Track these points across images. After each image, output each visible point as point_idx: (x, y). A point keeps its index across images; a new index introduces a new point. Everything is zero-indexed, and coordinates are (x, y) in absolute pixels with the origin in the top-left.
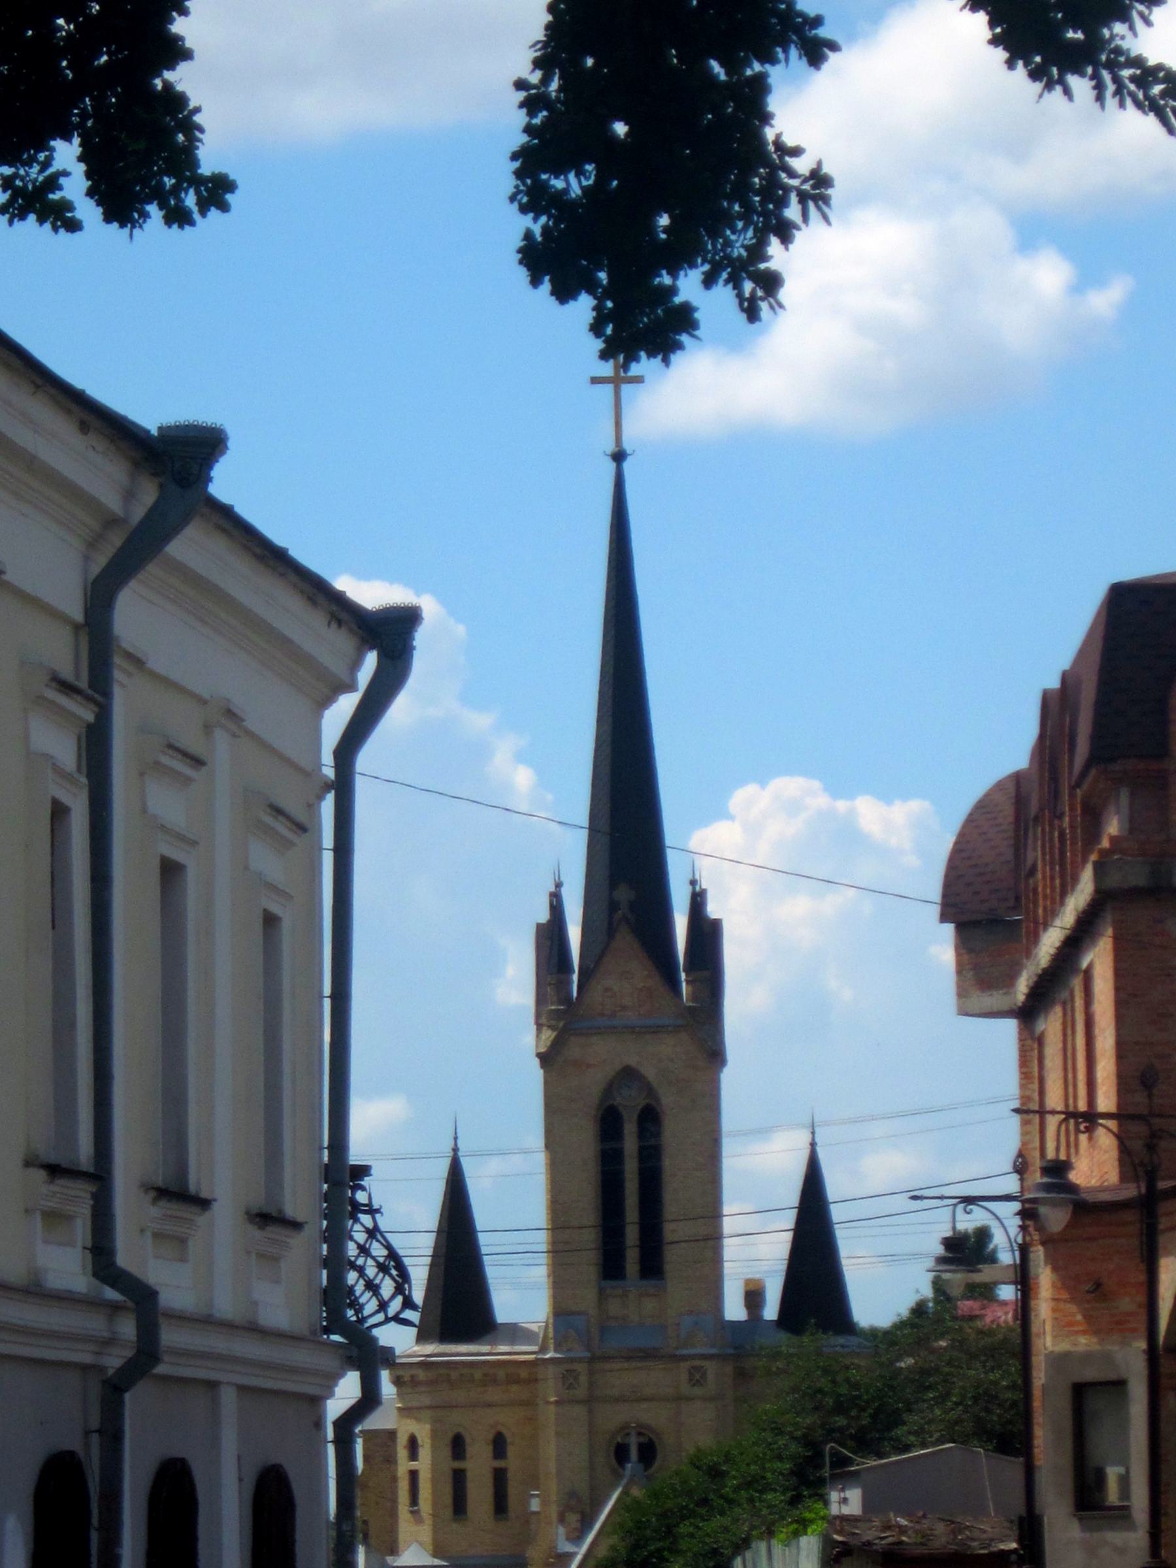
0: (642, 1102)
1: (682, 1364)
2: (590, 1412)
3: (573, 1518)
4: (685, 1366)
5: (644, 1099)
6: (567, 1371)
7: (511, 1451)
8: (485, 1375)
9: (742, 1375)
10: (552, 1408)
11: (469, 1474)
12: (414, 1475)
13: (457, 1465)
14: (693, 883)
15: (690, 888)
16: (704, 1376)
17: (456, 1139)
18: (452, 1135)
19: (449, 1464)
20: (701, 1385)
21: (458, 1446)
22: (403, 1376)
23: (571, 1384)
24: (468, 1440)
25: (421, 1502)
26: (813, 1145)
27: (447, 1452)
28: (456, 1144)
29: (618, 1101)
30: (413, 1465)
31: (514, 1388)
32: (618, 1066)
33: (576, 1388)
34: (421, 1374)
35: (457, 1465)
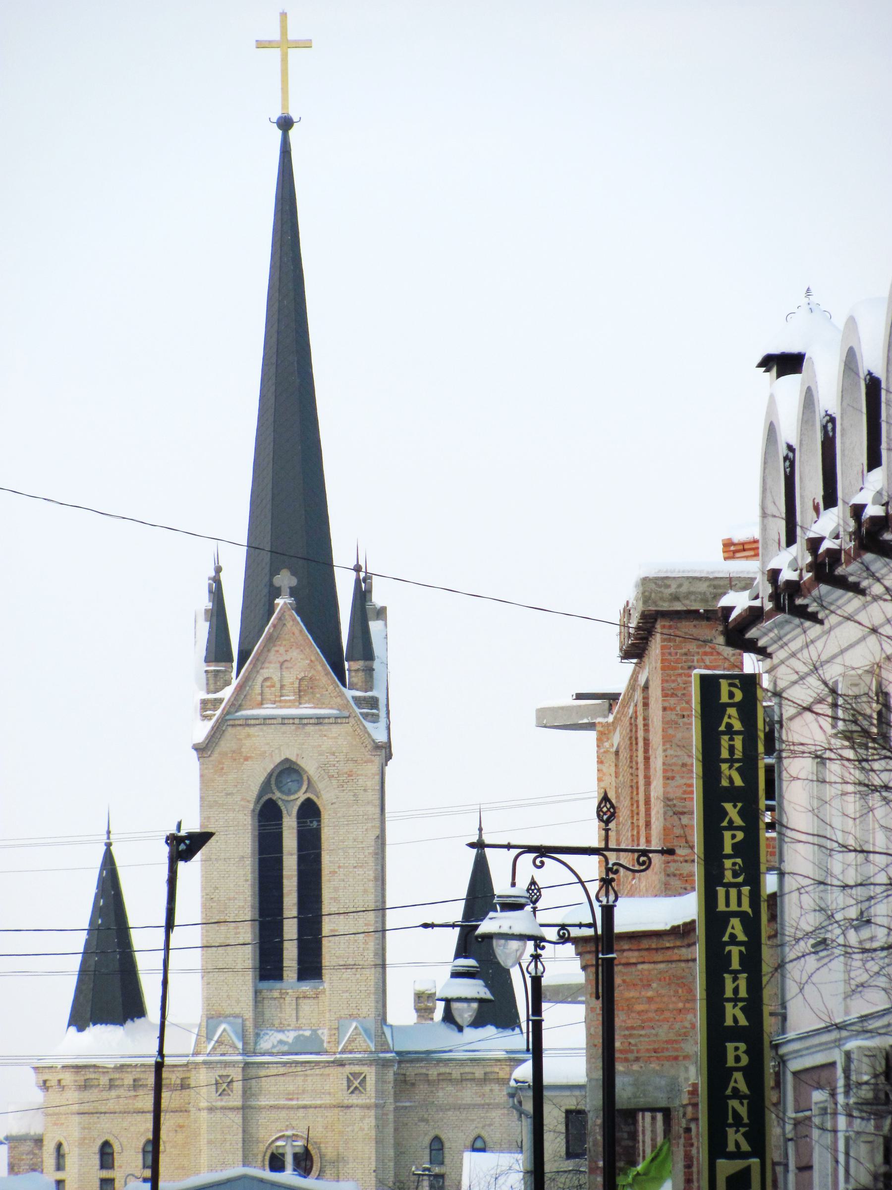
0: (301, 796)
2: (244, 1119)
5: (305, 792)
6: (219, 1076)
8: (135, 1080)
9: (403, 1084)
10: (204, 1114)
13: (106, 1174)
18: (106, 829)
20: (361, 1092)
21: (106, 1155)
23: (224, 1090)
24: (116, 1148)
29: (277, 795)
30: (60, 1175)
32: (278, 760)
33: (229, 1095)
34: (68, 1078)
35: (106, 1174)
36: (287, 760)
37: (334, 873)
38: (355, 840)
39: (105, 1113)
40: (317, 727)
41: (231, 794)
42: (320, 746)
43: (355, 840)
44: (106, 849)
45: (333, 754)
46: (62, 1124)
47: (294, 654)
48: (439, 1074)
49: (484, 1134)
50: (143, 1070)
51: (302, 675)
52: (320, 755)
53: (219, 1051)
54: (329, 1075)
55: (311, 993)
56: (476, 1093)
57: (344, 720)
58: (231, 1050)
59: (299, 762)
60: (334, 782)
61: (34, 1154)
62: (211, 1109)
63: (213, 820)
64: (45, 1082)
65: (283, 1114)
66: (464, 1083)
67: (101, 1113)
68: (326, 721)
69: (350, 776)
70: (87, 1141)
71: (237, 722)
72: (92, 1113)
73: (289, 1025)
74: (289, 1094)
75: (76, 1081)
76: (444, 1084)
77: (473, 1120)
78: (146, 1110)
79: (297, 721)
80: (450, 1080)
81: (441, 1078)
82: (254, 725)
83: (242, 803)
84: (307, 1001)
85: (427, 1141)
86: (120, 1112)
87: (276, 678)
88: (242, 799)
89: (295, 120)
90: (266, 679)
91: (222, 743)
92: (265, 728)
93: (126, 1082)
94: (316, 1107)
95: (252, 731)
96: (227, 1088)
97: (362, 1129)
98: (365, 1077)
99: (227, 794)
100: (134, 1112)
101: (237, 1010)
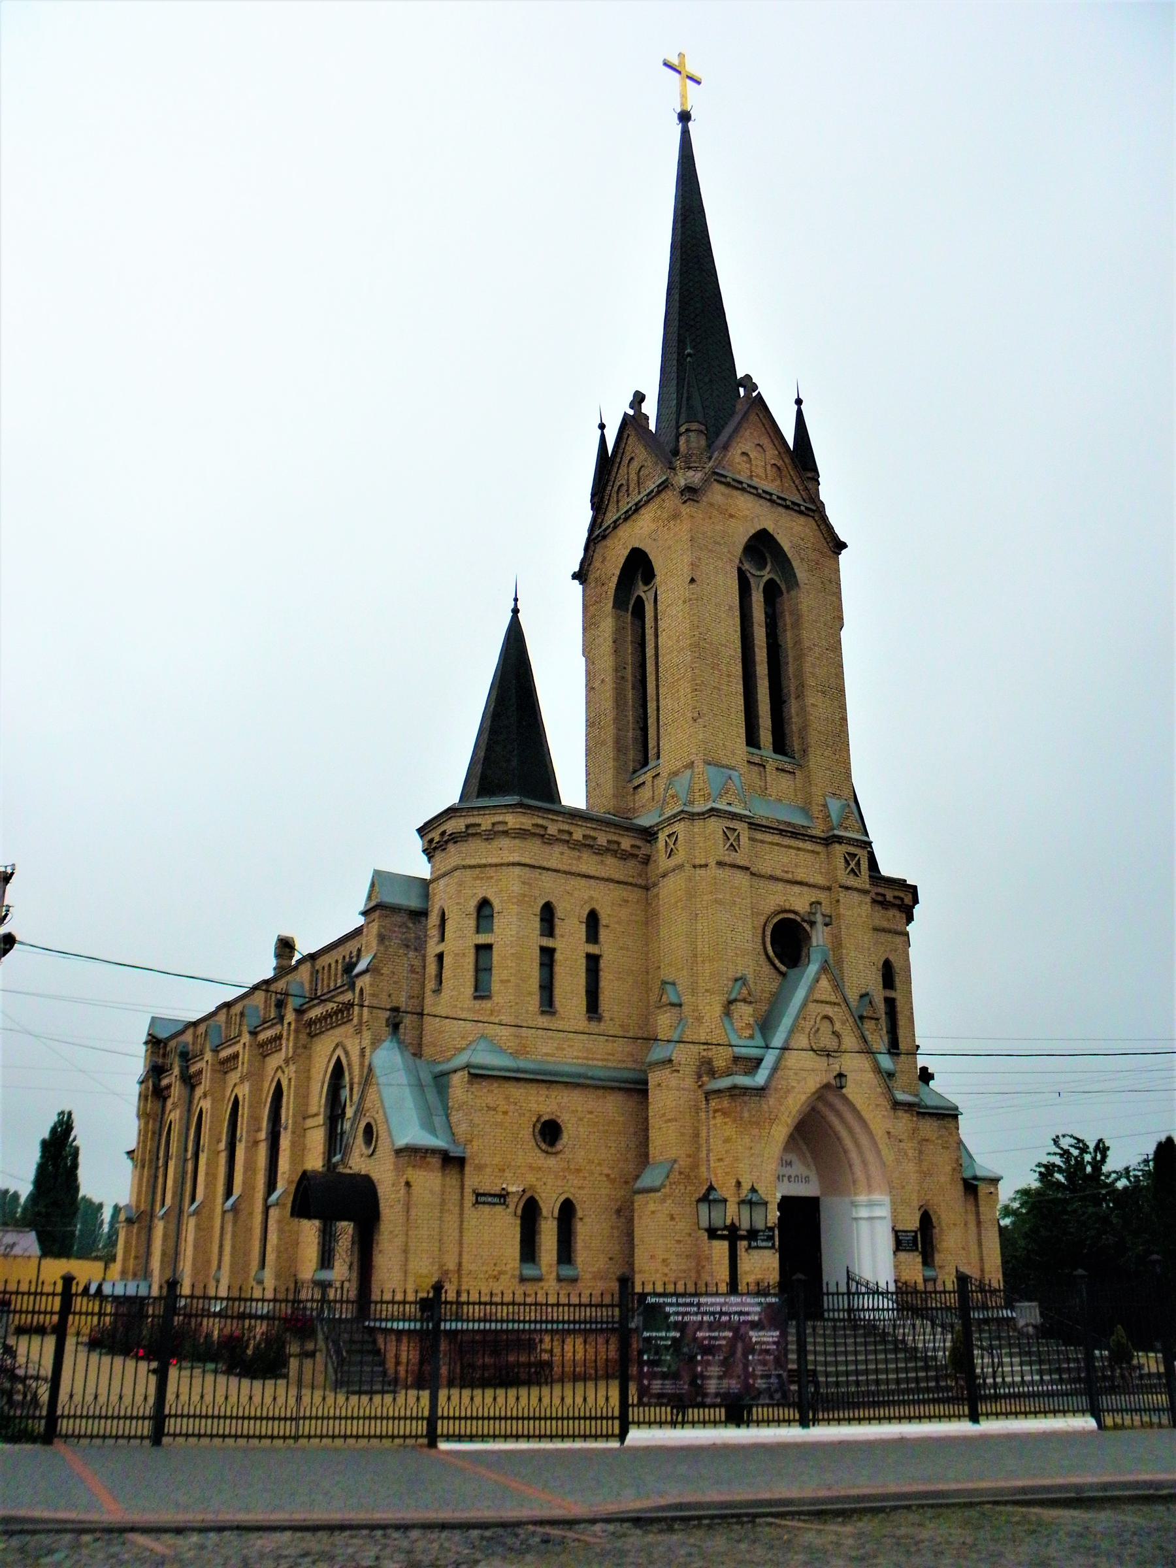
0: (767, 574)
1: (837, 846)
3: (744, 1012)
4: (839, 850)
7: (603, 934)
11: (558, 956)
14: (799, 402)
15: (796, 407)
16: (858, 864)
17: (516, 600)
19: (536, 940)
22: (479, 825)
23: (732, 845)
24: (559, 912)
25: (495, 987)
27: (536, 923)
28: (516, 605)
29: (746, 566)
30: (483, 939)
31: (610, 860)
32: (759, 528)
35: (547, 942)
37: (811, 649)
39: (548, 869)
40: (788, 512)
41: (719, 543)
42: (792, 529)
44: (512, 617)
45: (803, 540)
46: (491, 877)
47: (765, 441)
49: (891, 958)
50: (594, 826)
51: (773, 462)
54: (818, 853)
55: (788, 767)
56: (883, 917)
59: (776, 536)
61: (407, 927)
62: (720, 864)
64: (468, 827)
65: (780, 886)
67: (544, 868)
68: (796, 508)
69: (817, 564)
70: (526, 899)
71: (723, 479)
72: (533, 867)
73: (771, 796)
74: (783, 866)
75: (522, 824)
77: (882, 944)
78: (592, 873)
79: (774, 497)
82: (737, 488)
83: (729, 555)
86: (565, 873)
88: (729, 552)
89: (693, 118)
90: (743, 453)
91: (709, 494)
92: (746, 495)
93: (575, 836)
95: (736, 493)
97: (859, 916)
98: (859, 860)
99: (716, 543)
100: (579, 875)
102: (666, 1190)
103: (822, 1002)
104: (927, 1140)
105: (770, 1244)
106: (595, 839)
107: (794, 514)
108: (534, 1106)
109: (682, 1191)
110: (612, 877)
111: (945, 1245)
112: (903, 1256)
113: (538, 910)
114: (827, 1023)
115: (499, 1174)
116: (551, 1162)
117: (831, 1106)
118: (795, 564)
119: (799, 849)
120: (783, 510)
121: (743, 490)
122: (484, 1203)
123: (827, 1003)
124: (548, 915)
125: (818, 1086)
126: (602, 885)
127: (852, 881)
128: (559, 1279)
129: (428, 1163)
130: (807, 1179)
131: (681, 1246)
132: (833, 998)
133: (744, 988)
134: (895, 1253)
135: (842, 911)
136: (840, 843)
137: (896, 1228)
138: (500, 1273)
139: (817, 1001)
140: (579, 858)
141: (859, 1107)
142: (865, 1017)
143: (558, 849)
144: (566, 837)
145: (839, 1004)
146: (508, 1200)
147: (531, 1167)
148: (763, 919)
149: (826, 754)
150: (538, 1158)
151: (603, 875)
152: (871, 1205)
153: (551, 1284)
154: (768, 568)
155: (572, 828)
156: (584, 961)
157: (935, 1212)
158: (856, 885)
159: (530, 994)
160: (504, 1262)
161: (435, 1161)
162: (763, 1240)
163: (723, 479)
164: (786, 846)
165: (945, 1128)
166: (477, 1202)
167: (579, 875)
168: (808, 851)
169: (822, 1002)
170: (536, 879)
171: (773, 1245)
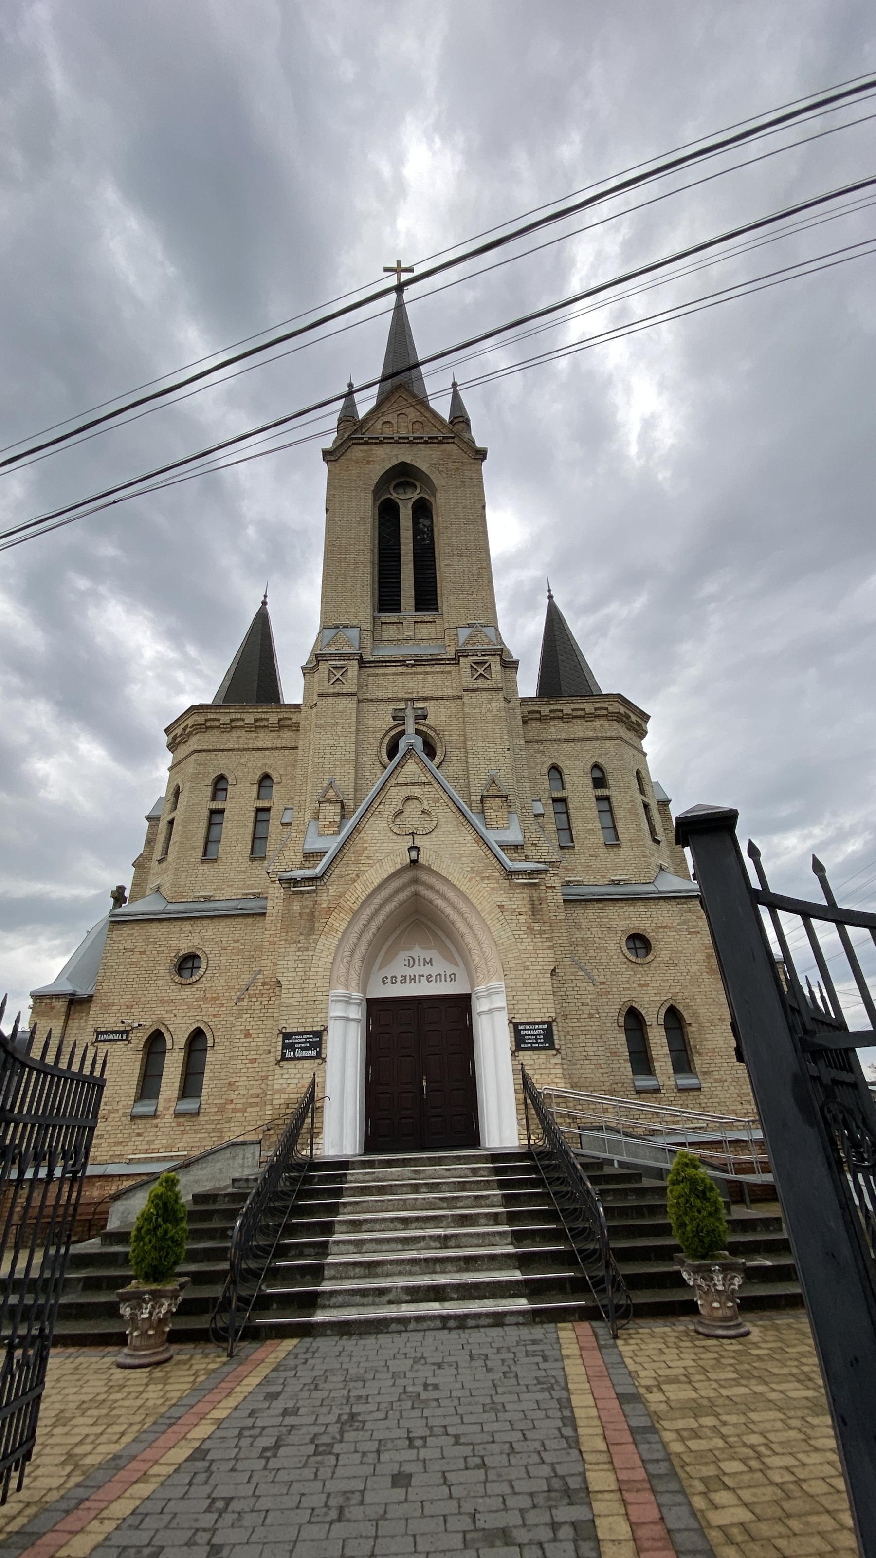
0: (416, 496)
3: (331, 812)
12: (171, 822)
26: (550, 597)
27: (209, 792)
29: (394, 496)
32: (395, 462)
35: (215, 805)
36: (403, 463)
37: (447, 528)
38: (464, 508)
39: (223, 750)
40: (427, 446)
43: (464, 508)
48: (551, 711)
52: (430, 459)
53: (334, 647)
54: (450, 672)
57: (450, 440)
58: (346, 647)
59: (413, 463)
60: (444, 475)
63: (337, 496)
64: (174, 738)
66: (575, 720)
67: (219, 750)
68: (436, 441)
71: (361, 441)
72: (209, 751)
76: (556, 722)
77: (588, 751)
78: (265, 746)
80: (562, 718)
81: (552, 715)
82: (376, 443)
84: (424, 625)
85: (545, 769)
86: (239, 750)
87: (393, 422)
92: (384, 446)
94: (437, 699)
96: (341, 678)
100: (253, 749)
101: (355, 623)
102: (245, 1004)
103: (406, 784)
104: (665, 927)
105: (314, 1053)
106: (267, 719)
107: (436, 445)
108: (174, 943)
109: (266, 1003)
110: (288, 745)
111: (709, 1045)
112: (526, 1057)
113: (209, 781)
114: (413, 805)
115: (129, 1011)
116: (187, 993)
117: (431, 887)
118: (432, 477)
119: (427, 673)
120: (420, 446)
121: (381, 443)
122: (105, 1041)
123: (413, 784)
124: (220, 784)
125: (399, 866)
126: (276, 753)
127: (480, 684)
128: (177, 1115)
129: (53, 1008)
130: (453, 977)
131: (256, 1065)
132: (423, 779)
133: (331, 790)
134: (513, 1053)
135: (467, 711)
136: (467, 656)
137: (514, 1021)
138: (110, 1112)
139: (401, 785)
140: (256, 737)
141: (455, 882)
142: (487, 796)
143: (235, 734)
144: (240, 723)
145: (430, 784)
146: (130, 1035)
147: (163, 1001)
148: (379, 735)
149: (461, 597)
150: (175, 992)
151: (279, 746)
152: (490, 993)
153: (167, 1119)
154: (418, 491)
155: (244, 716)
156: (253, 814)
157: (688, 1007)
158: (486, 686)
159: (194, 848)
160: (117, 1099)
161: (60, 1006)
162: (303, 1049)
163: (361, 441)
164: (411, 674)
165: (690, 911)
166: (97, 1041)
167: (253, 749)
168: (437, 673)
169: (406, 784)
170: (211, 760)
171: (319, 1056)
